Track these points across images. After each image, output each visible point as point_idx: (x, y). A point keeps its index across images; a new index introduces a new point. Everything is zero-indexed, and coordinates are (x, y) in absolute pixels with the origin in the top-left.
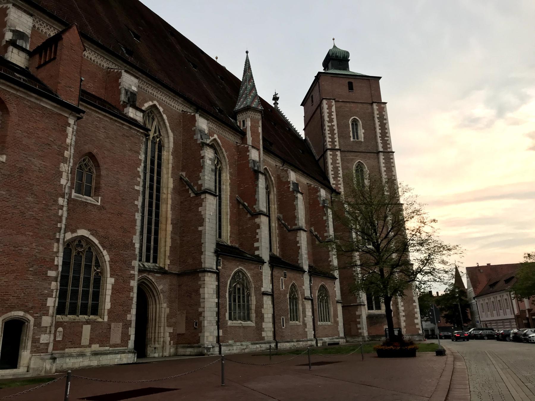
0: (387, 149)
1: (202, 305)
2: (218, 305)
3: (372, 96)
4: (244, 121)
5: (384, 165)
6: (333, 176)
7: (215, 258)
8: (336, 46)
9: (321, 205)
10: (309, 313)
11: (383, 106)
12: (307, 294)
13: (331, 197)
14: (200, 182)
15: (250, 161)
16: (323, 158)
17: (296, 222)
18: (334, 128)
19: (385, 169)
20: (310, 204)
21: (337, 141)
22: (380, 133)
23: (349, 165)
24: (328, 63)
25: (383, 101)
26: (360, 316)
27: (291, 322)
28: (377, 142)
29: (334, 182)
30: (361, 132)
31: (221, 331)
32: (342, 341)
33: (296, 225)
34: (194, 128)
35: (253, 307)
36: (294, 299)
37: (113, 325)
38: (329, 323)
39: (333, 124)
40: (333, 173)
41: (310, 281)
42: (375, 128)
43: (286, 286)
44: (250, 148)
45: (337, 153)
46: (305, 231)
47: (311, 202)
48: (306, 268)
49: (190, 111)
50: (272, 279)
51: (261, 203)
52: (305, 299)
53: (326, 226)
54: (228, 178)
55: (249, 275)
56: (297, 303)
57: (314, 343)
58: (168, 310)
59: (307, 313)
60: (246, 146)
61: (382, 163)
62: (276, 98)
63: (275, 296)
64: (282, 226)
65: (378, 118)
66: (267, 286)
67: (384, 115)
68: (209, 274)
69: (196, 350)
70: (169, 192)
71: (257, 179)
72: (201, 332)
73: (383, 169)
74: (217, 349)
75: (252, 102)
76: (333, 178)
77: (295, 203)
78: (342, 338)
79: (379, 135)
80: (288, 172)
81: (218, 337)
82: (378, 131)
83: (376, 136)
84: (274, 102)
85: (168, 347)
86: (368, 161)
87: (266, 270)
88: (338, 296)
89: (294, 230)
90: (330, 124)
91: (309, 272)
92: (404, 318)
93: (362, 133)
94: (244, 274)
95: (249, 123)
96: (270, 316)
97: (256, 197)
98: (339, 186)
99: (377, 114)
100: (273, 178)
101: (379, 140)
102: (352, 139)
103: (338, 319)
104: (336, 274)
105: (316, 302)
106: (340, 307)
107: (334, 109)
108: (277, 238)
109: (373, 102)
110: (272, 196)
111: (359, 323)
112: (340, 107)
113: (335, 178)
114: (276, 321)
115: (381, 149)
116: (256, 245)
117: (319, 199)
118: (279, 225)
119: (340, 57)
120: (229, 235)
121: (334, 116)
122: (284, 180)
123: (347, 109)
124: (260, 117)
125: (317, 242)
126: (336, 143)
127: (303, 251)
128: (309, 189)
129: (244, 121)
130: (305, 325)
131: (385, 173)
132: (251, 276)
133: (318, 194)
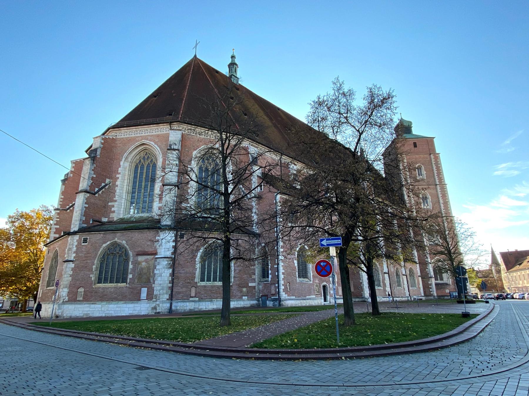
10: (406, 283)
12: (404, 273)
19: (441, 195)
25: (437, 152)
26: (431, 284)
28: (435, 179)
32: (424, 298)
35: (381, 280)
36: (397, 275)
37: (339, 287)
42: (433, 170)
52: (403, 275)
56: (399, 277)
57: (409, 298)
61: (439, 192)
66: (386, 270)
67: (438, 162)
69: (361, 299)
72: (362, 291)
73: (440, 195)
78: (423, 296)
79: (436, 174)
82: (435, 172)
83: (434, 175)
88: (419, 274)
96: (389, 284)
99: (434, 161)
103: (420, 286)
105: (408, 277)
106: (420, 278)
109: (431, 154)
111: (431, 288)
114: (391, 287)
130: (404, 289)
131: (441, 198)
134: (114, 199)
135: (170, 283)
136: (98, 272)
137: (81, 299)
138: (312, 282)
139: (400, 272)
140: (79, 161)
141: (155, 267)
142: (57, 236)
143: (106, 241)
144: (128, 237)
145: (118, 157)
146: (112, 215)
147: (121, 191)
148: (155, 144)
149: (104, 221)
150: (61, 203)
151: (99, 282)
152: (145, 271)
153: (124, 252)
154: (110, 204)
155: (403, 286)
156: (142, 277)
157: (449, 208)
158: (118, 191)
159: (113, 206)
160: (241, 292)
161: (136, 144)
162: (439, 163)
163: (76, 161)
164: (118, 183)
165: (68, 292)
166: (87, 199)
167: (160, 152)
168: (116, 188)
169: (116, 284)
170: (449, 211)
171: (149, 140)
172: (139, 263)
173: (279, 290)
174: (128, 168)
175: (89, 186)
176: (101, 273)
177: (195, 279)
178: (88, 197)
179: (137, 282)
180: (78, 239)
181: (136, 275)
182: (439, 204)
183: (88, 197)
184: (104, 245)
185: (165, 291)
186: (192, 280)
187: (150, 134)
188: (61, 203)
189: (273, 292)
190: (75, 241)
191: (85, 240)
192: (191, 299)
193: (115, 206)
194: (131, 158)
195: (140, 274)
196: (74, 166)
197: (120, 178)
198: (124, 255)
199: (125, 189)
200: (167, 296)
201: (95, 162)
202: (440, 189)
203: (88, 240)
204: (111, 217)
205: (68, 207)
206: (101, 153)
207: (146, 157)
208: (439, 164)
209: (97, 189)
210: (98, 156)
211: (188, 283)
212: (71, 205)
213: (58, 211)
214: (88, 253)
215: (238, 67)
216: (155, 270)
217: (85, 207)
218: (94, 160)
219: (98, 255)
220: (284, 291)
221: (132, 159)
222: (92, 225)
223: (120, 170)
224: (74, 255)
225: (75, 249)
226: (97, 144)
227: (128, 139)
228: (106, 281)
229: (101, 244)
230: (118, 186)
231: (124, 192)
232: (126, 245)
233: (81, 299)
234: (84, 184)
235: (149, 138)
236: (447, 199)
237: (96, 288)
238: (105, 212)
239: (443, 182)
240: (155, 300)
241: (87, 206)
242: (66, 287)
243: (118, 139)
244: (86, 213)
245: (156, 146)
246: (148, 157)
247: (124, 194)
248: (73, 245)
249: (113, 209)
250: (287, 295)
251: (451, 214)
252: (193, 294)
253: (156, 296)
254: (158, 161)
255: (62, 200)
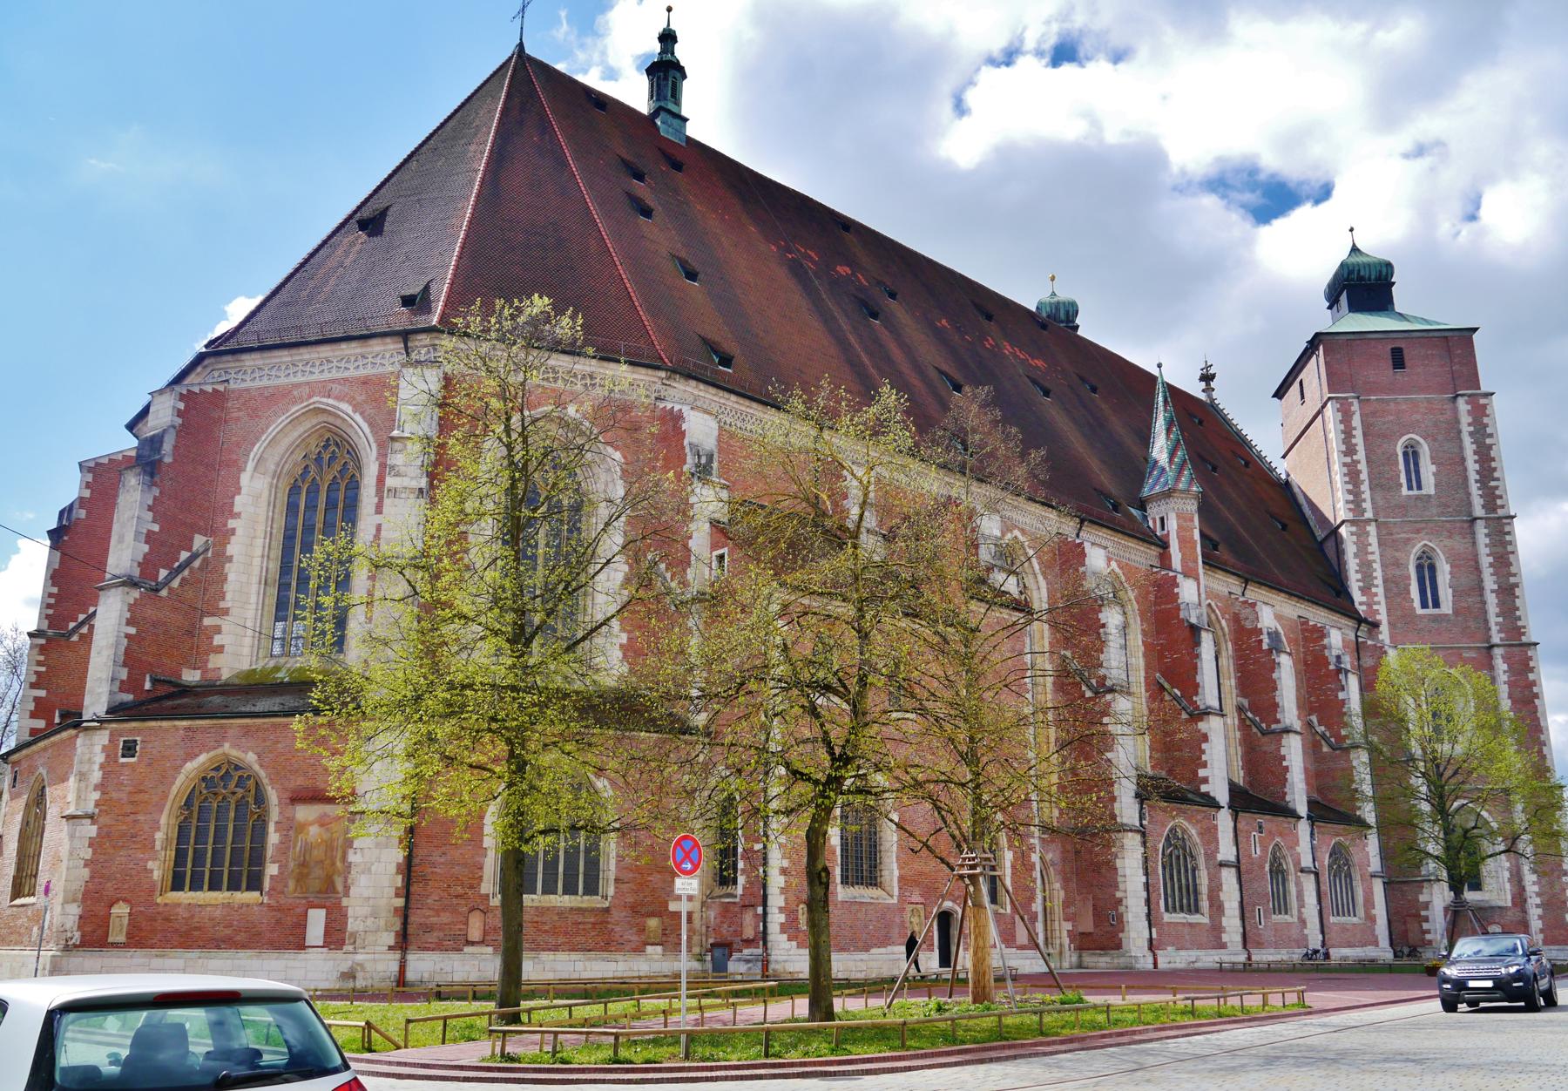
0: (1494, 510)
1: (1121, 886)
2: (1147, 886)
3: (1453, 379)
4: (1162, 519)
5: (1487, 551)
6: (1361, 584)
7: (1137, 807)
8: (1359, 245)
9: (1332, 667)
11: (1482, 401)
12: (1306, 861)
13: (1357, 637)
14: (1102, 672)
15: (1182, 607)
16: (1333, 538)
17: (1278, 716)
18: (1359, 467)
19: (1491, 559)
20: (1306, 663)
21: (1369, 500)
22: (1478, 472)
23: (1397, 554)
24: (1340, 294)
25: (1484, 388)
27: (1274, 917)
29: (1364, 599)
30: (1428, 470)
31: (1154, 930)
33: (1278, 721)
34: (1082, 569)
35: (1204, 889)
36: (1278, 872)
38: (1355, 920)
39: (1355, 457)
40: (1359, 576)
41: (1312, 834)
42: (1463, 460)
43: (1264, 849)
44: (1180, 578)
45: (1368, 528)
46: (1296, 732)
47: (1309, 658)
48: (1302, 810)
49: (1069, 527)
50: (1236, 836)
51: (1207, 691)
52: (1302, 871)
53: (1345, 714)
54: (1140, 643)
55: (1194, 832)
58: (1062, 893)
59: (1306, 899)
60: (1171, 574)
62: (1207, 378)
63: (1243, 868)
64: (1248, 723)
65: (1471, 434)
66: (1227, 851)
67: (1486, 426)
68: (1130, 834)
70: (1048, 690)
71: (1198, 644)
72: (1123, 931)
73: (1486, 561)
74: (1150, 959)
75: (1177, 479)
76: (1360, 588)
77: (1275, 676)
79: (1473, 476)
80: (1257, 608)
81: (1151, 940)
82: (1472, 466)
83: (1466, 479)
84: (1203, 383)
85: (1067, 953)
86: (1448, 542)
87: (1224, 820)
88: (1375, 864)
89: (1273, 732)
90: (1348, 460)
91: (1309, 818)
92: (1539, 911)
93: (1430, 474)
94: (1184, 831)
95: (1172, 525)
97: (1198, 679)
98: (1375, 607)
99: (1469, 425)
100: (1224, 623)
101: (1474, 489)
102: (1405, 491)
103: (1374, 912)
104: (1368, 813)
105: (1325, 878)
106: (1378, 888)
107: (1356, 421)
108: (1239, 748)
110: (1223, 661)
112: (1374, 414)
113: (1365, 590)
114: (1247, 915)
115: (1479, 511)
116: (1202, 773)
117: (1327, 653)
118: (1242, 721)
119: (1370, 279)
120: (1148, 754)
121: (1359, 439)
122: (1248, 625)
123: (1391, 418)
124: (1195, 507)
125: (1325, 749)
126: (1364, 505)
127: (1295, 775)
128: (1303, 631)
129: (1162, 519)
130: (1303, 922)
131: (1491, 570)
132: (1200, 834)
133: (1326, 641)
134: (222, 605)
135: (397, 895)
136: (173, 853)
137: (122, 938)
138: (895, 900)
139: (1289, 860)
140: (105, 461)
141: (349, 843)
142: (40, 724)
143: (196, 751)
144: (264, 741)
145: (234, 457)
146: (214, 661)
147: (244, 578)
148: (355, 412)
149: (191, 679)
150: (51, 612)
151: (177, 885)
152: (318, 854)
153: (253, 792)
154: (207, 621)
155: (1300, 912)
156: (308, 874)
157: (1518, 609)
158: (231, 577)
159: (218, 629)
160: (642, 930)
161: (293, 410)
162: (1489, 430)
163: (97, 464)
164: (231, 549)
165: (81, 917)
166: (131, 608)
167: (371, 440)
168: (227, 565)
169: (228, 894)
170: (1519, 623)
171: (338, 398)
172: (302, 827)
173: (765, 927)
174: (265, 494)
175: (140, 564)
176: (180, 857)
177: (483, 885)
178: (136, 599)
179: (295, 891)
180: (107, 742)
181: (292, 865)
182: (1482, 595)
183: (136, 599)
184: (190, 766)
185: (382, 923)
186: (471, 887)
187: (340, 375)
188: (51, 612)
189: (749, 933)
190: (98, 749)
191: (129, 749)
192: (467, 949)
193: (224, 628)
194: (277, 459)
195: (304, 864)
196: (90, 480)
197: (239, 532)
198: (251, 800)
199: (256, 571)
200: (390, 939)
201: (157, 479)
202: (1486, 535)
203: (138, 748)
204: (210, 665)
205: (72, 625)
206: (176, 447)
207: (326, 456)
208: (1491, 436)
209: (163, 573)
210: (168, 460)
211: (457, 897)
212: (81, 617)
213: (42, 641)
214: (141, 791)
215: (684, 76)
216: (351, 852)
217: (128, 636)
218: (152, 475)
219: (171, 797)
220: (784, 928)
221: (278, 465)
222: (152, 695)
223: (239, 502)
224: (96, 795)
225: (96, 776)
226: (164, 416)
227: (266, 394)
228: (196, 886)
229: (178, 762)
230: (234, 559)
231: (255, 579)
232: (256, 767)
233: (122, 938)
234: (124, 554)
235: (336, 388)
236: (1515, 575)
237: (166, 905)
238: (192, 648)
239: (1503, 507)
240: (350, 948)
241: (132, 631)
242: (74, 901)
243: (233, 391)
244: (132, 658)
245: (358, 417)
246: (333, 458)
247: (254, 588)
248: (90, 761)
249: (217, 640)
250: (794, 943)
251: (1524, 634)
252: (475, 933)
253: (354, 935)
254: (365, 471)
255: (52, 601)
